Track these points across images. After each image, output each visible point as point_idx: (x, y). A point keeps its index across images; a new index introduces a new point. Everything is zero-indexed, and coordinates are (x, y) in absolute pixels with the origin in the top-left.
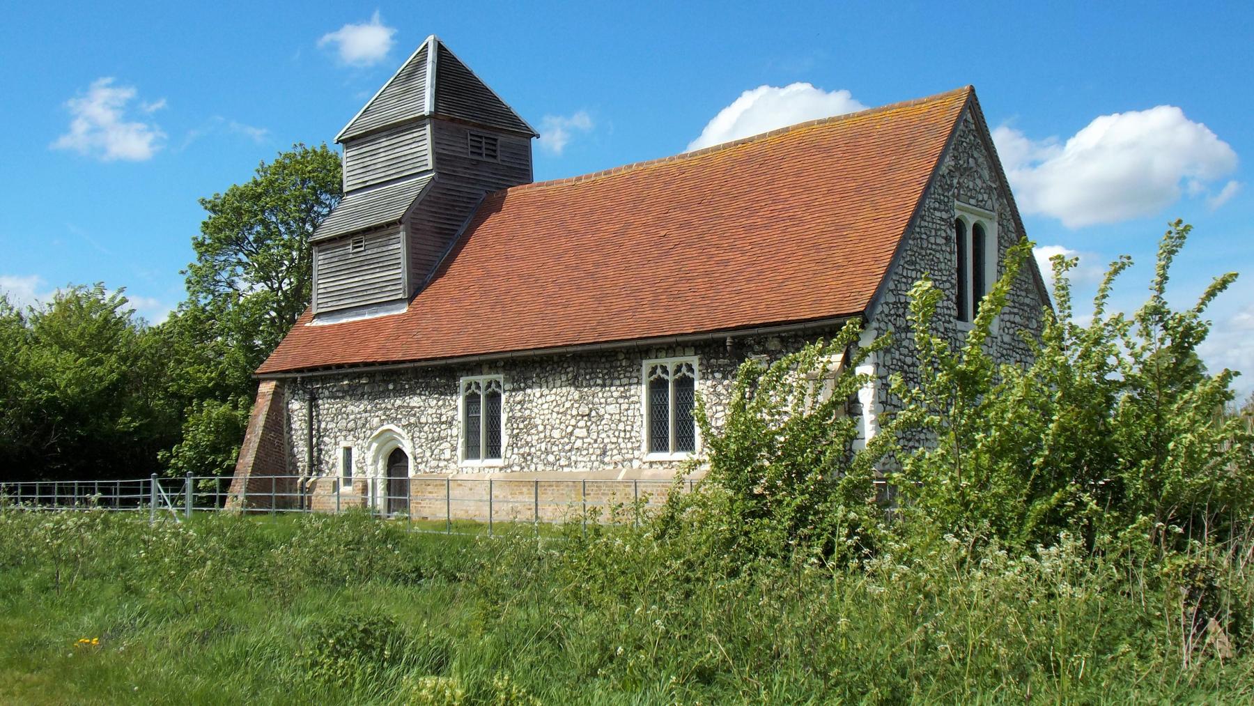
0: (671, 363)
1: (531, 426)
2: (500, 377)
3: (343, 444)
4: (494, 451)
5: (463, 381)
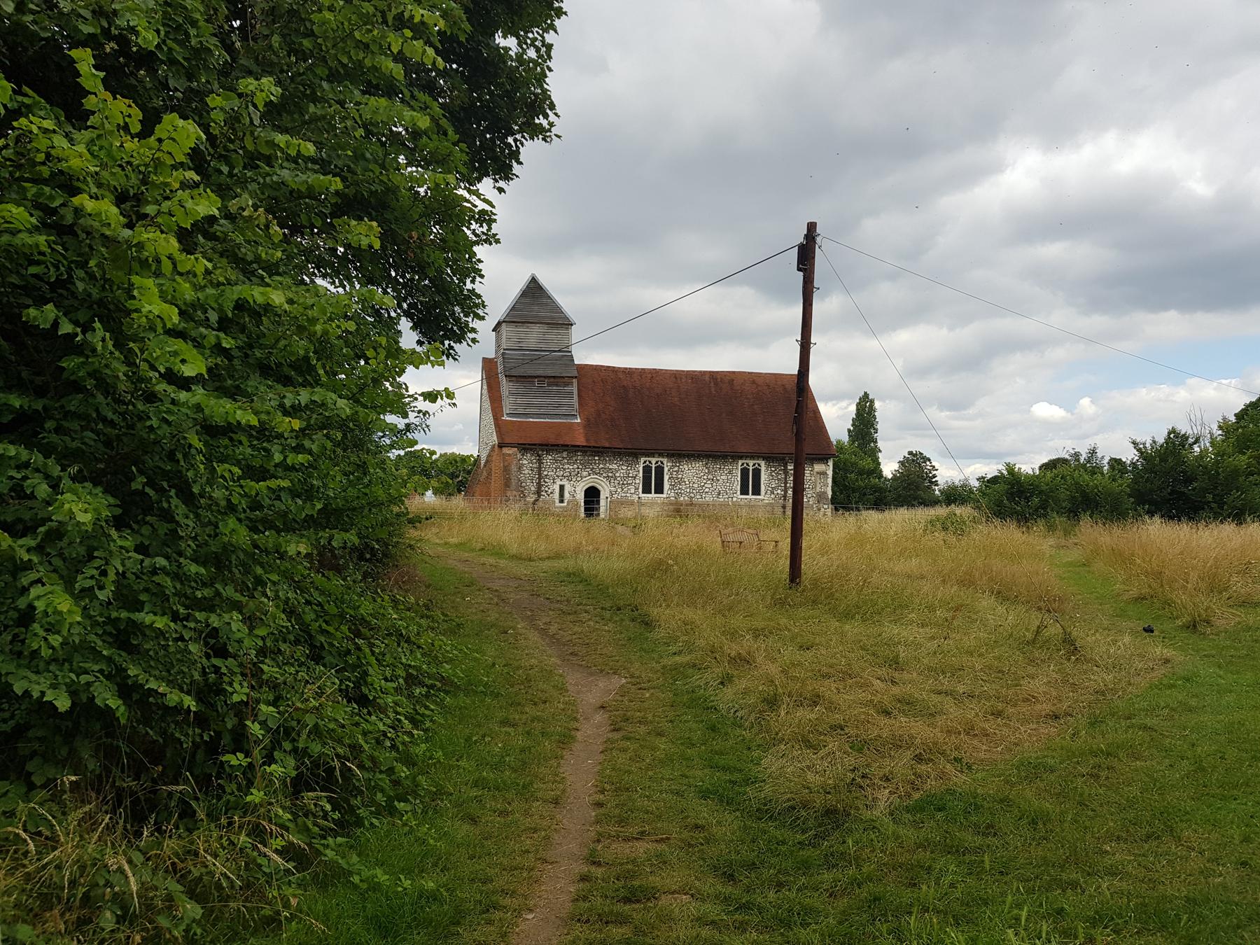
0: (751, 463)
1: (681, 481)
2: (665, 461)
3: (559, 483)
4: (659, 490)
5: (643, 460)
